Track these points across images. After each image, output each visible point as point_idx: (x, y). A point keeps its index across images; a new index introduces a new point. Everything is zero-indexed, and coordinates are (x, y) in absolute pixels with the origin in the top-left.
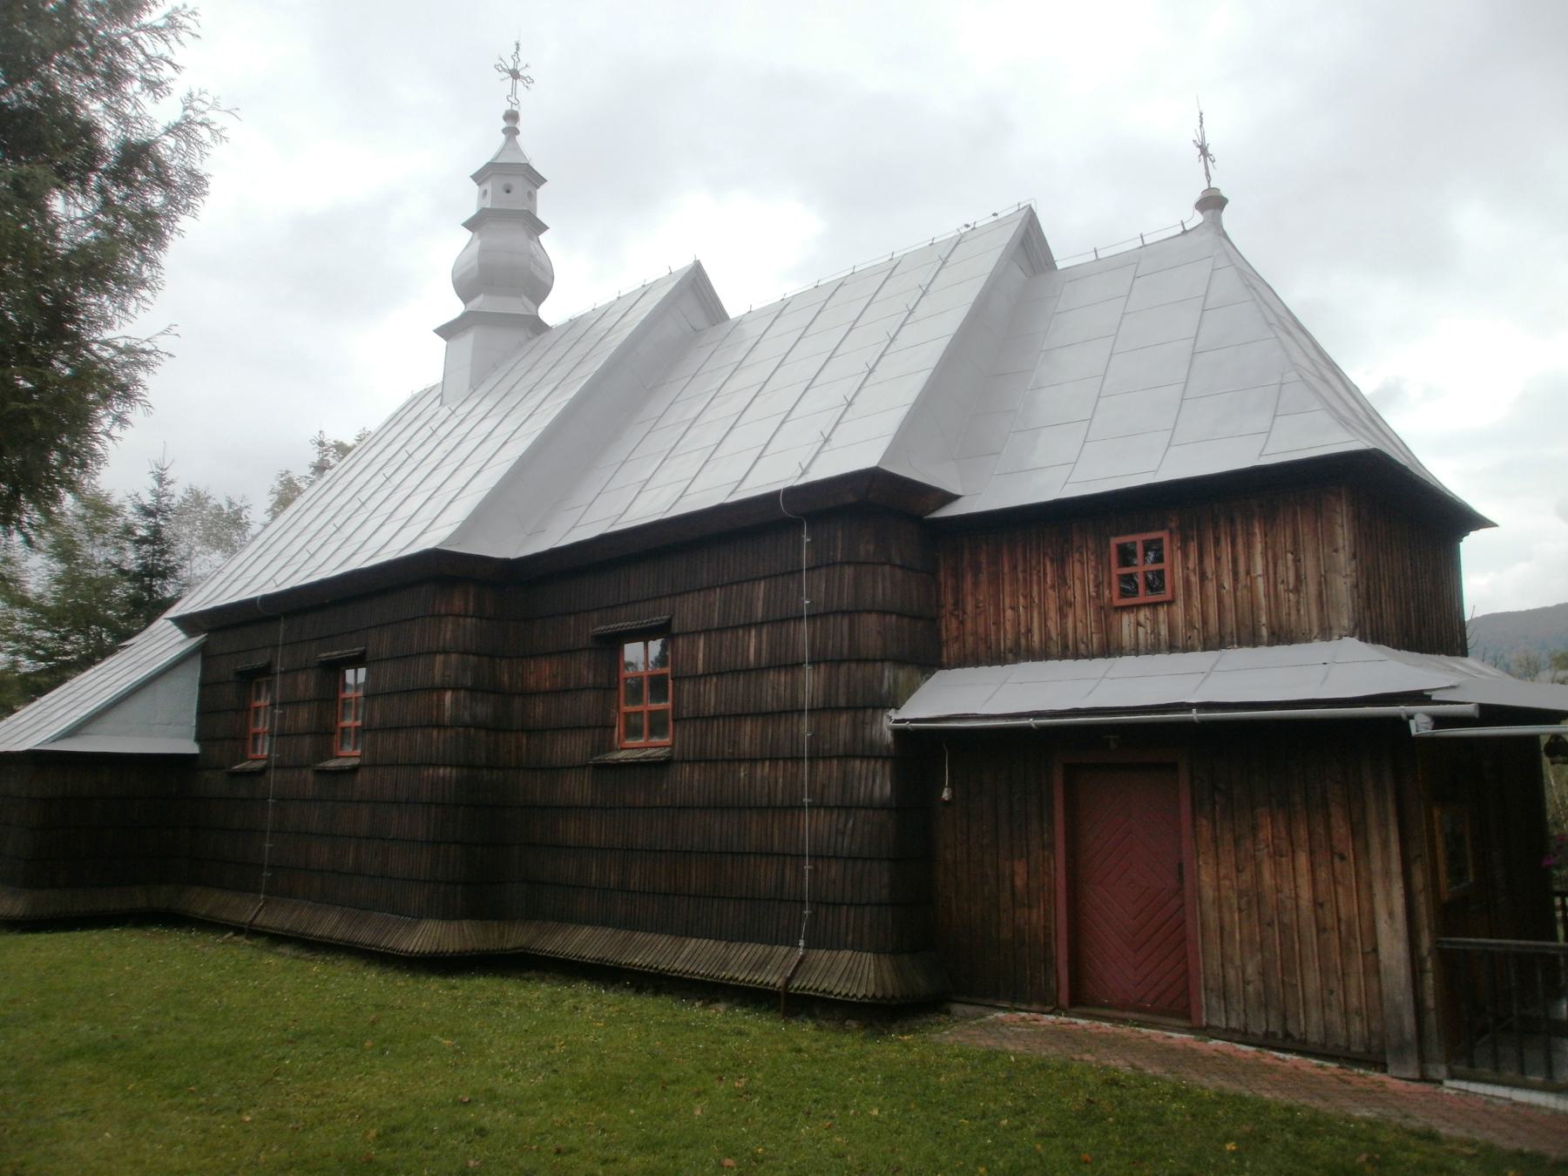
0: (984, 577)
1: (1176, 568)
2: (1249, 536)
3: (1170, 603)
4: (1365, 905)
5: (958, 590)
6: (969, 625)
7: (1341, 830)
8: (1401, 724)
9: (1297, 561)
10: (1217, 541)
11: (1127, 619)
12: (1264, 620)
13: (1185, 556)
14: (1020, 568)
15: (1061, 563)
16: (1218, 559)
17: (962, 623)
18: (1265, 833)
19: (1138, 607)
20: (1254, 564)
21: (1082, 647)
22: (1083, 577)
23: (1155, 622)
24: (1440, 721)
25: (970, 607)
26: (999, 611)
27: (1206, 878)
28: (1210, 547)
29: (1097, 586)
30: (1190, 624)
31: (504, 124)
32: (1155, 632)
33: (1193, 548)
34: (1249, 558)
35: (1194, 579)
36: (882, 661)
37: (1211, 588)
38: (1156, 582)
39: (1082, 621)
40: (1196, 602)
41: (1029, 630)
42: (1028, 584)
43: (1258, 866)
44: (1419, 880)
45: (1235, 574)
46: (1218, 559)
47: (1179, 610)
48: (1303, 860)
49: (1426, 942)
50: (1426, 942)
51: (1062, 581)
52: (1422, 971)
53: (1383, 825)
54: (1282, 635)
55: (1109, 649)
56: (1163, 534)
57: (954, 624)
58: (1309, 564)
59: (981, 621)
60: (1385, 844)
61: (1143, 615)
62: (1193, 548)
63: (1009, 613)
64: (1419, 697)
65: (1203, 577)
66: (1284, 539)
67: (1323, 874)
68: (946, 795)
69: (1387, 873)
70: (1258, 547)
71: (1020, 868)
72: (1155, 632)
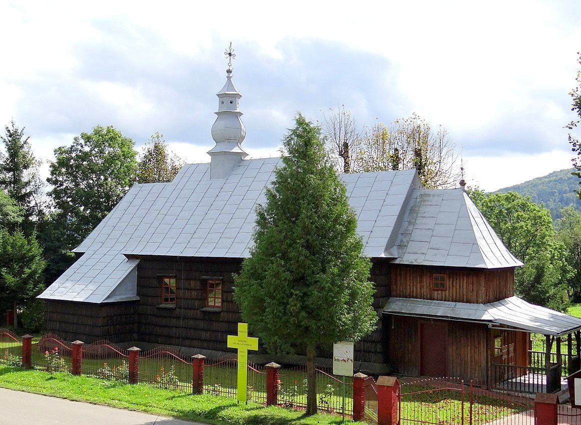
0: (402, 278)
1: (448, 283)
2: (463, 279)
3: (445, 291)
4: (480, 357)
5: (396, 279)
6: (398, 288)
7: (476, 343)
8: (487, 325)
9: (473, 286)
10: (456, 279)
11: (436, 292)
12: (465, 297)
13: (449, 281)
14: (411, 277)
15: (421, 277)
16: (456, 283)
17: (397, 287)
18: (462, 342)
19: (438, 290)
20: (463, 285)
21: (425, 297)
22: (426, 281)
23: (442, 294)
24: (493, 326)
25: (399, 284)
26: (406, 286)
27: (450, 350)
28: (455, 280)
29: (430, 284)
30: (449, 296)
31: (227, 74)
32: (442, 296)
33: (451, 279)
34: (463, 285)
35: (451, 286)
36: (380, 297)
37: (454, 288)
38: (443, 285)
39: (425, 291)
40: (451, 291)
41: (413, 291)
42: (413, 280)
43: (461, 348)
44: (489, 352)
45: (460, 287)
46: (456, 283)
47: (447, 292)
48: (469, 348)
49: (489, 365)
50: (489, 365)
51: (421, 282)
52: (489, 370)
53: (484, 342)
54: (468, 301)
55: (432, 299)
56: (445, 275)
57: (395, 287)
58: (475, 286)
59: (401, 288)
60: (484, 346)
61: (440, 292)
62: (451, 279)
63: (408, 287)
64: (490, 321)
65: (453, 286)
66: (470, 280)
67: (473, 351)
68: (393, 328)
69: (484, 351)
70: (465, 282)
71: (410, 345)
72: (442, 296)
